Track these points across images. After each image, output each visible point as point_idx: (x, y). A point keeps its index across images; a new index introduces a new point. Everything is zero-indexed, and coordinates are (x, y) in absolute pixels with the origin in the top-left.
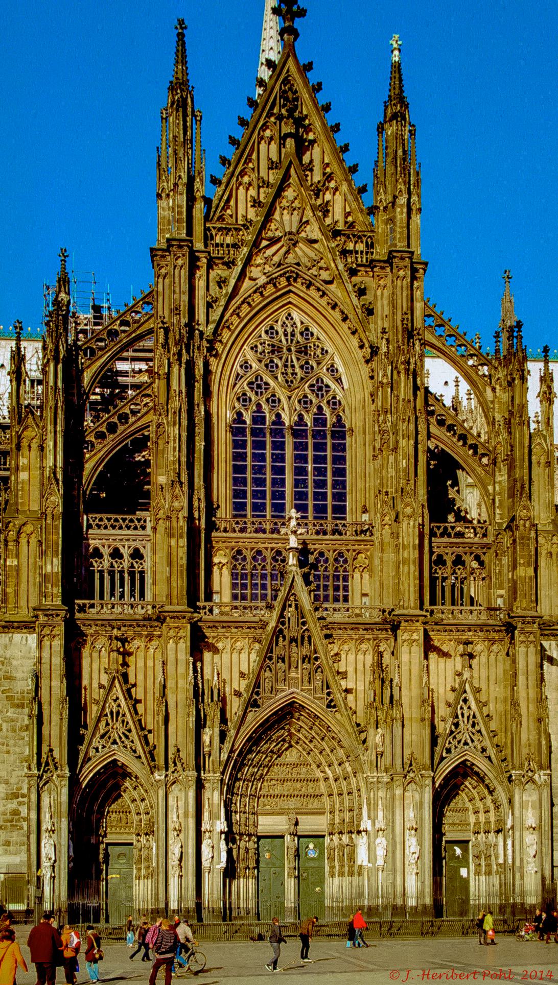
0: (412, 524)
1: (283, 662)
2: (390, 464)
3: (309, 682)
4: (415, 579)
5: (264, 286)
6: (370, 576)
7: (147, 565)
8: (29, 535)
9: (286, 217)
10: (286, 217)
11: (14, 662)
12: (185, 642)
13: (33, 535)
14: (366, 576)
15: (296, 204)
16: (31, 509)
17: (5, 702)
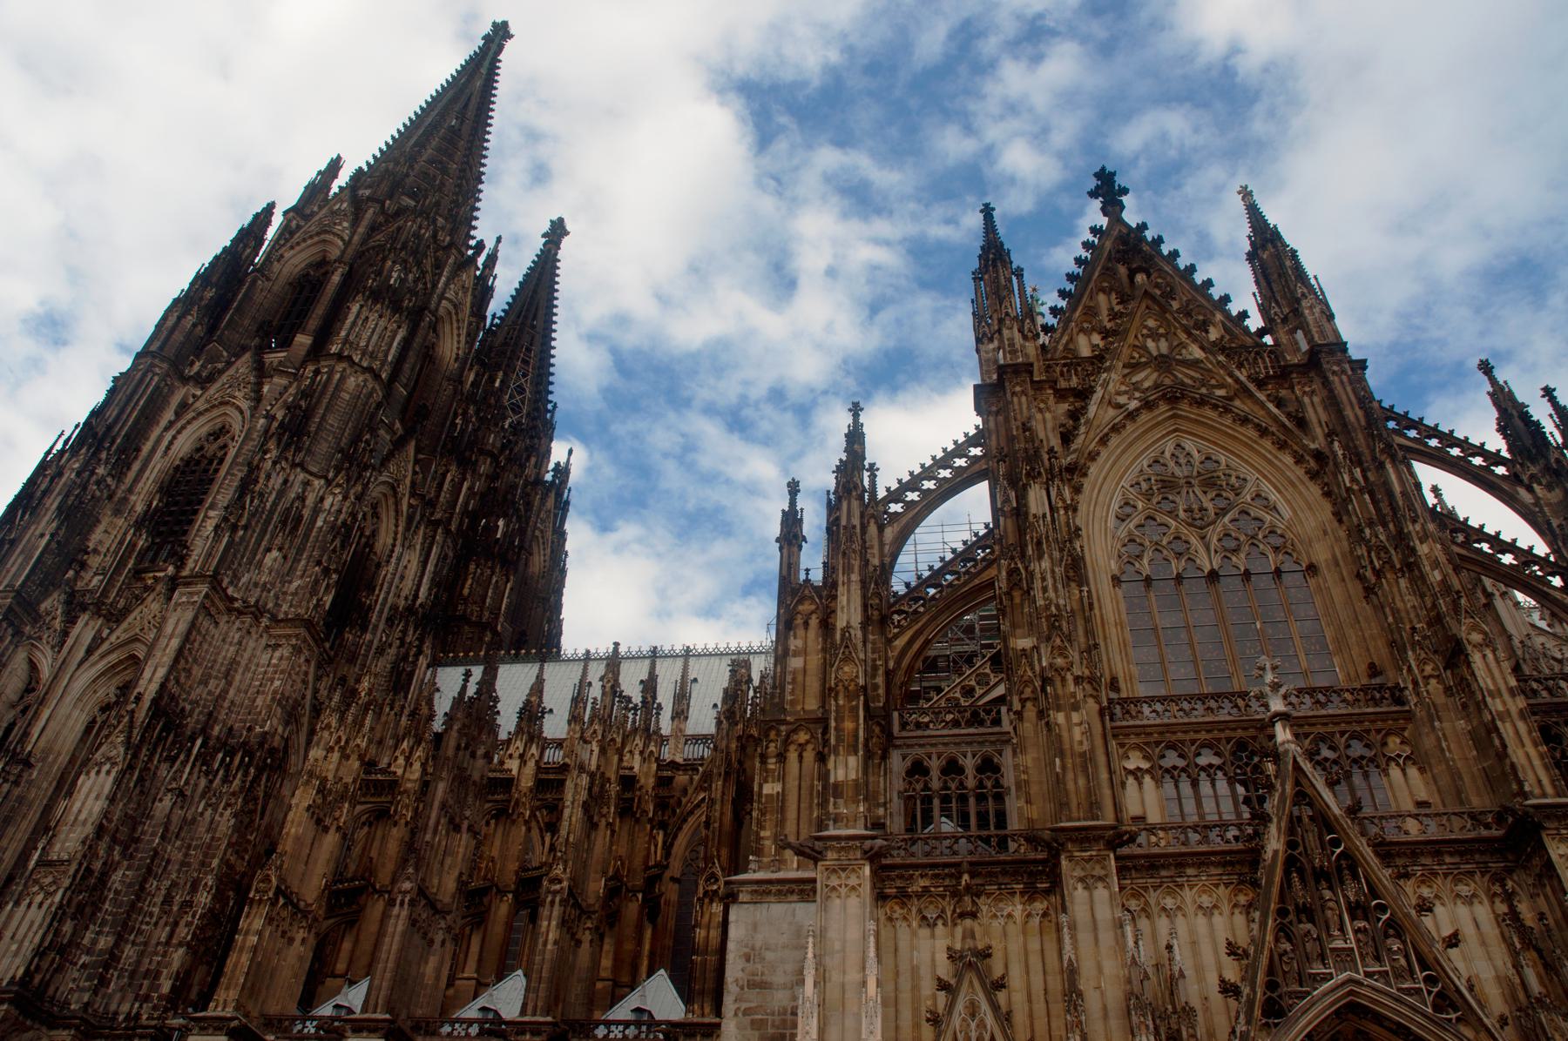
0: (1490, 656)
1: (1312, 920)
2: (1404, 590)
3: (1378, 958)
4: (1536, 745)
5: (1137, 410)
6: (1422, 770)
7: (1009, 779)
8: (802, 747)
9: (1150, 344)
10: (1150, 344)
11: (769, 956)
12: (1107, 887)
13: (810, 747)
14: (1413, 772)
15: (1161, 331)
16: (807, 707)
17: (749, 1032)
